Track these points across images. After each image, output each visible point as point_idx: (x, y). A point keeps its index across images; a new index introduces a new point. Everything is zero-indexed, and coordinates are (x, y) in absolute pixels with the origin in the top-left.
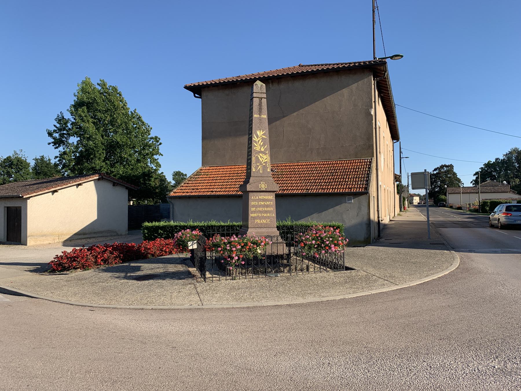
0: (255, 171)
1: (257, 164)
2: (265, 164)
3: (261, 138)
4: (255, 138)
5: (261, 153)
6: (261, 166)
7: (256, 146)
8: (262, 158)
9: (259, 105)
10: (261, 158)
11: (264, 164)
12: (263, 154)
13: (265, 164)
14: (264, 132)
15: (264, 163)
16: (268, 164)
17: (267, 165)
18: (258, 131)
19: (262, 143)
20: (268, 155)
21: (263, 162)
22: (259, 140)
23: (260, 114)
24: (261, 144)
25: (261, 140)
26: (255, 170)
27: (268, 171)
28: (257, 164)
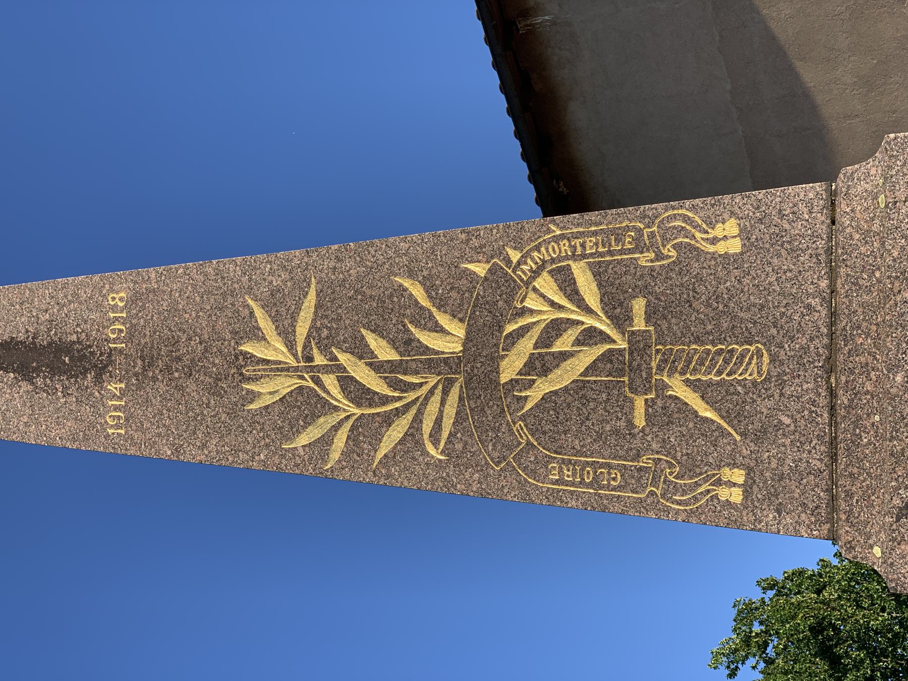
0: (739, 476)
1: (640, 421)
2: (639, 306)
3: (319, 360)
4: (326, 441)
5: (495, 360)
6: (669, 363)
7: (413, 434)
8: (554, 349)
9: (25, 372)
10: (564, 356)
11: (639, 324)
12: (510, 328)
13: (639, 306)
14: (259, 313)
15: (621, 320)
16: (639, 248)
17: (645, 259)
18: (254, 396)
19: (372, 340)
20: (515, 256)
21: (606, 338)
22: (347, 383)
23: (101, 371)
24: (393, 356)
25: (343, 358)
26: (727, 474)
27: (734, 246)
28: (640, 421)
